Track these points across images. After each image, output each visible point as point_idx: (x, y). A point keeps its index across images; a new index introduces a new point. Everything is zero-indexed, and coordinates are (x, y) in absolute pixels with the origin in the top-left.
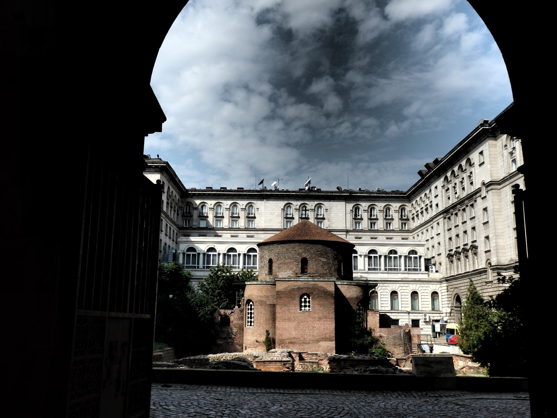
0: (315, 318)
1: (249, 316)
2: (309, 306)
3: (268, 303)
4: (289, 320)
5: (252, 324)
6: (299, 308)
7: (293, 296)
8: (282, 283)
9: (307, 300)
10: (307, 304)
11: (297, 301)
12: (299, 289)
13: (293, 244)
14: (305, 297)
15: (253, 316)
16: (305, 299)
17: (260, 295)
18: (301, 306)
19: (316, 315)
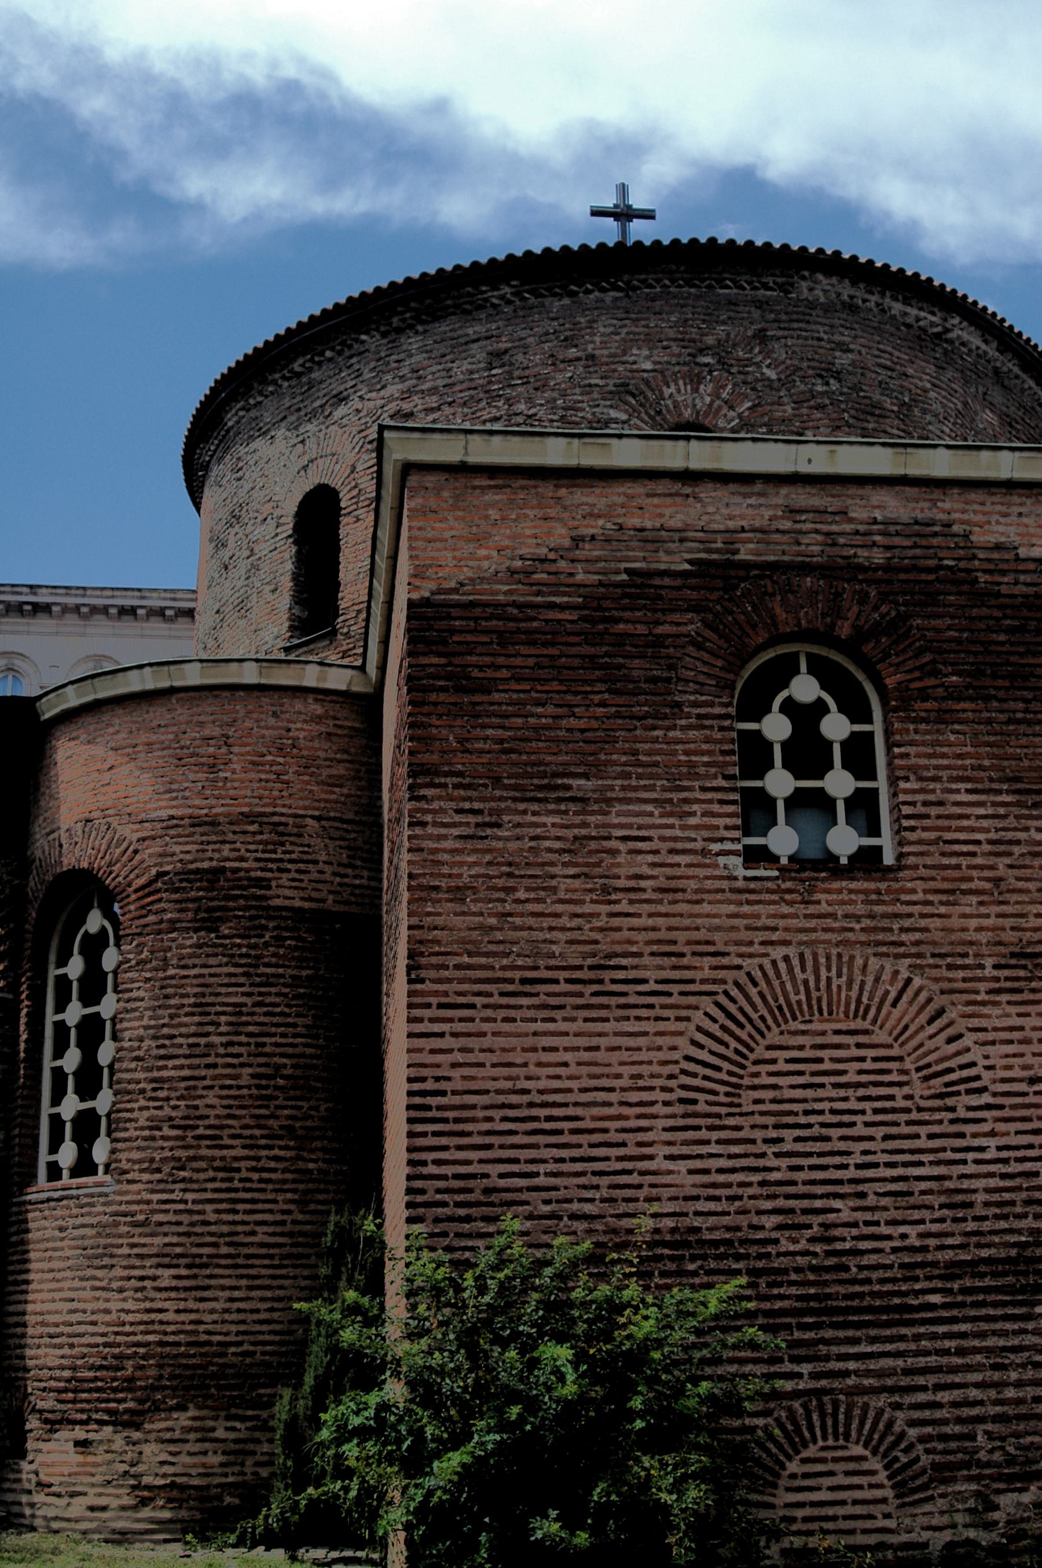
0: (954, 955)
1: (71, 1060)
2: (863, 808)
3: (285, 894)
4: (599, 981)
5: (100, 1152)
6: (727, 818)
7: (637, 667)
8: (492, 499)
9: (836, 727)
10: (839, 783)
11: (695, 739)
12: (720, 576)
13: (556, 305)
14: (805, 688)
15: (105, 1053)
16: (805, 717)
17: (199, 806)
18: (757, 810)
19: (973, 920)
